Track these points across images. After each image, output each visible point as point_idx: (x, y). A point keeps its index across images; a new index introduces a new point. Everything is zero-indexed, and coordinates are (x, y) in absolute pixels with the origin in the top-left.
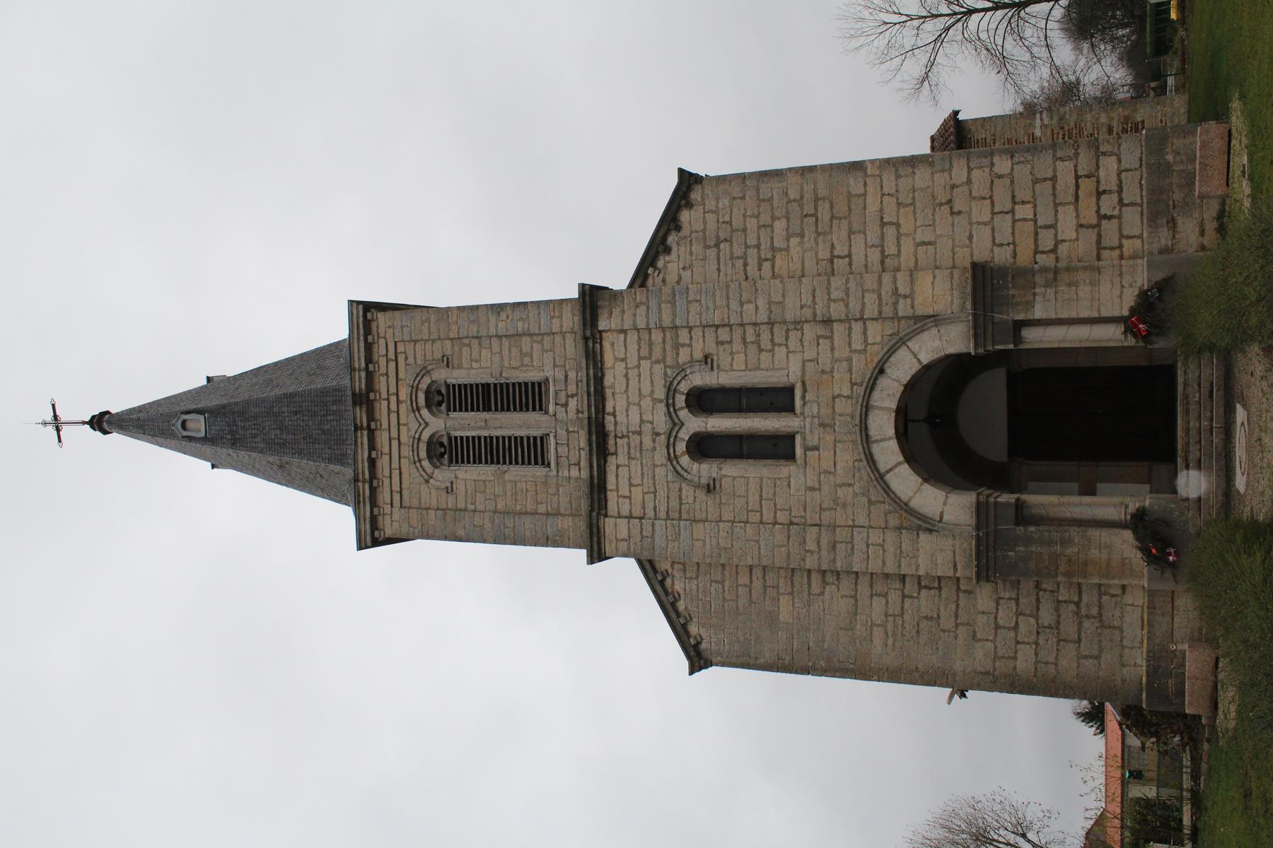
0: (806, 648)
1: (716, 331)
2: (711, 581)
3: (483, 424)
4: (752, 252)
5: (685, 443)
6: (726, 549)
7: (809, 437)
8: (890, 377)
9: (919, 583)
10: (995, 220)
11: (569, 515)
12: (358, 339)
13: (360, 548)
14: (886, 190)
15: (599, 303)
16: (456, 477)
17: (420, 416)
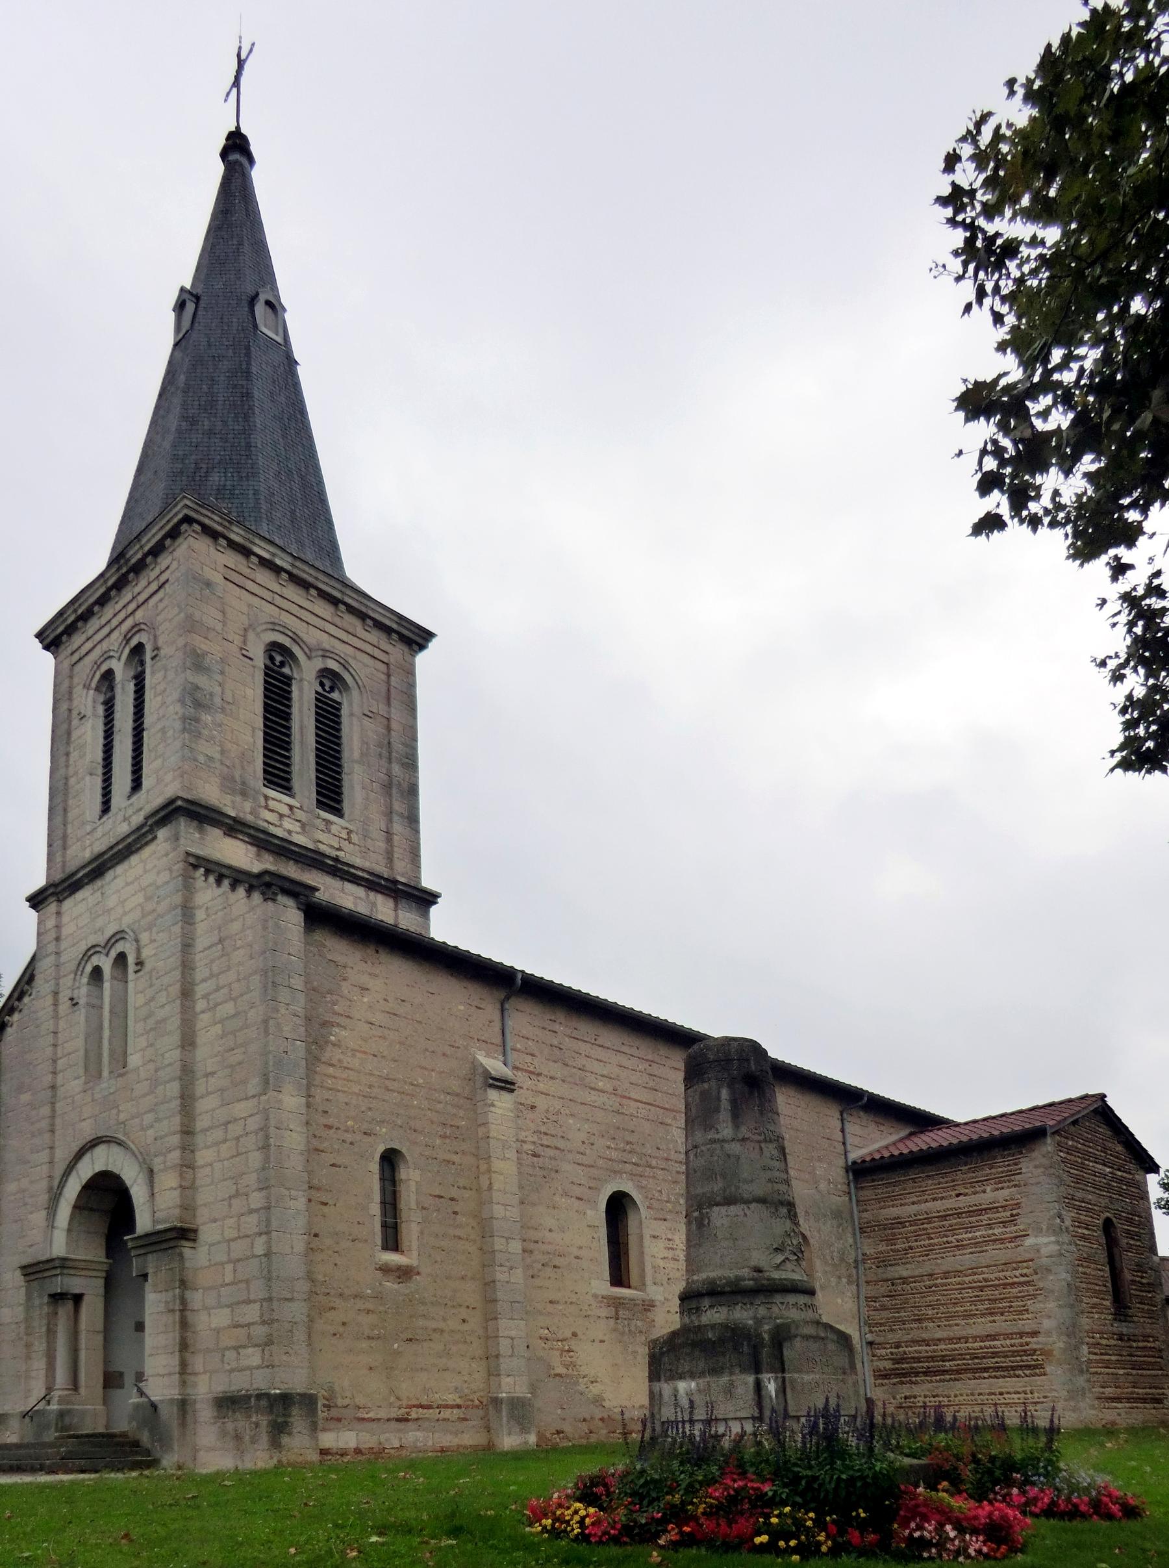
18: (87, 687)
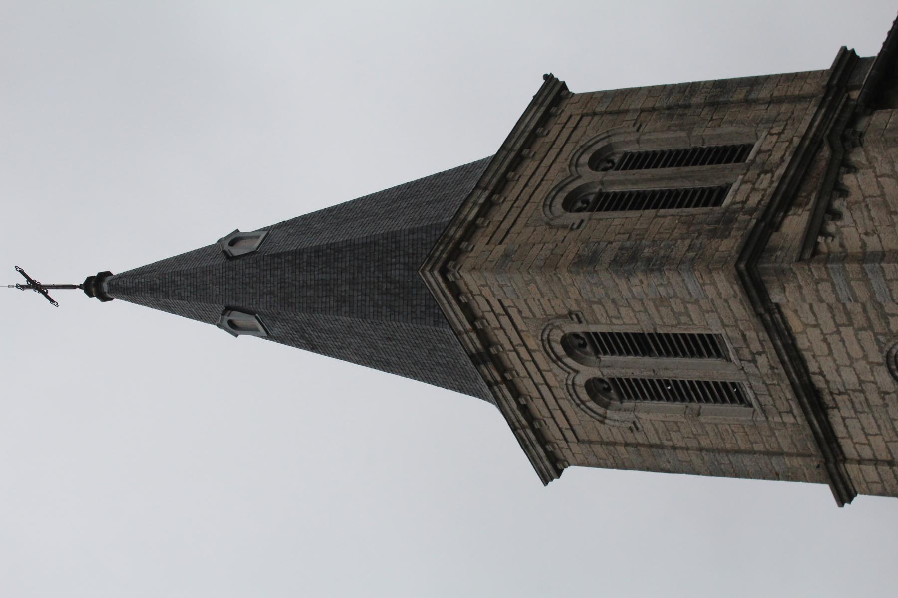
12: (450, 304)
13: (546, 483)
15: (764, 278)
18: (603, 419)
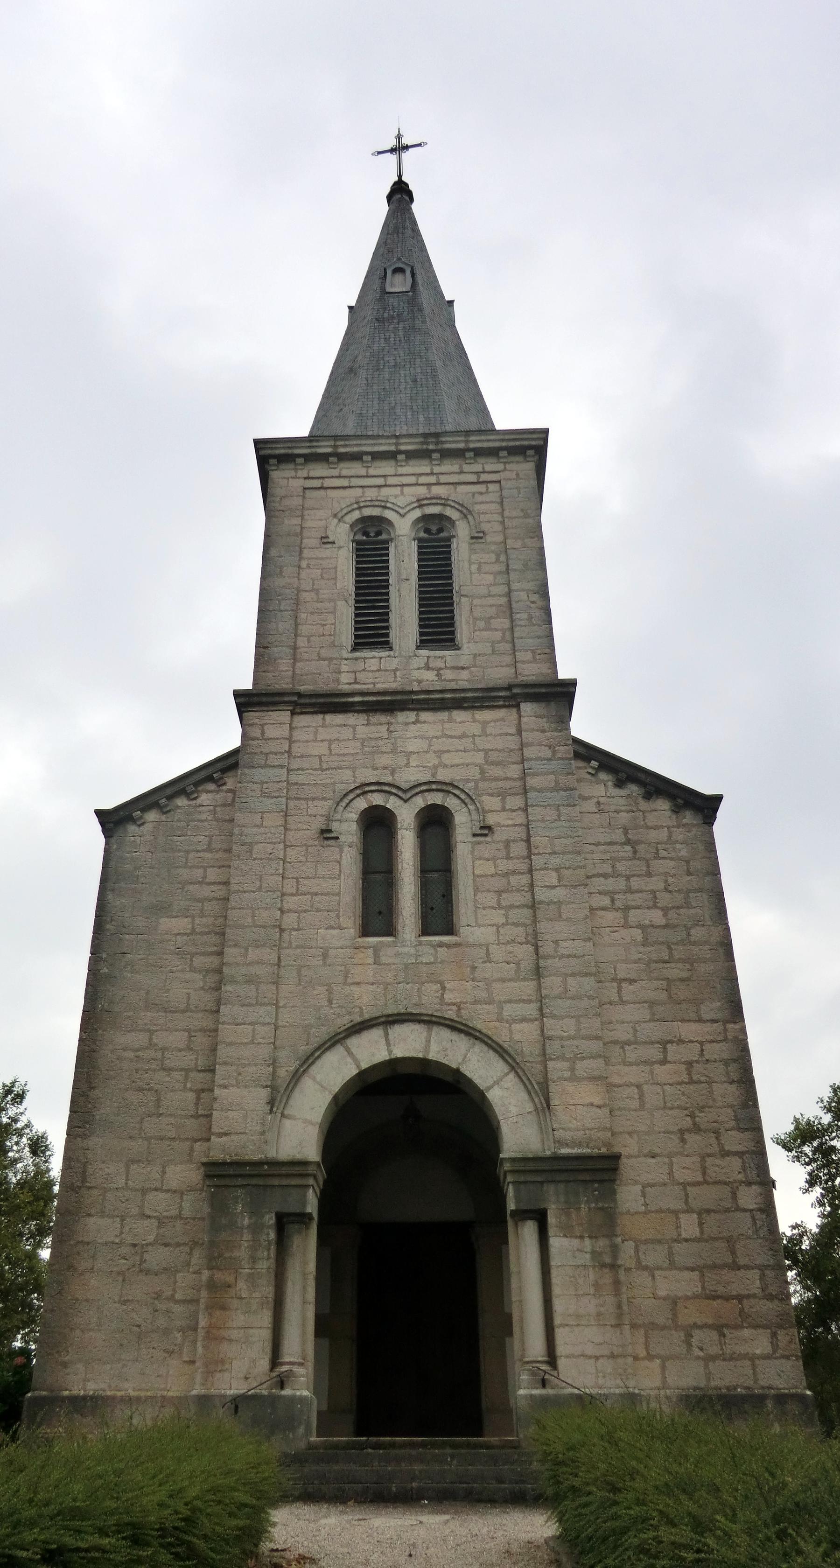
0: (125, 950)
1: (522, 840)
2: (211, 837)
3: (404, 577)
4: (622, 884)
5: (382, 804)
6: (251, 852)
7: (391, 951)
8: (468, 1051)
9: (203, 1091)
10: (676, 1187)
11: (294, 671)
12: (503, 440)
14: (707, 1047)
16: (340, 547)
17: (413, 509)
